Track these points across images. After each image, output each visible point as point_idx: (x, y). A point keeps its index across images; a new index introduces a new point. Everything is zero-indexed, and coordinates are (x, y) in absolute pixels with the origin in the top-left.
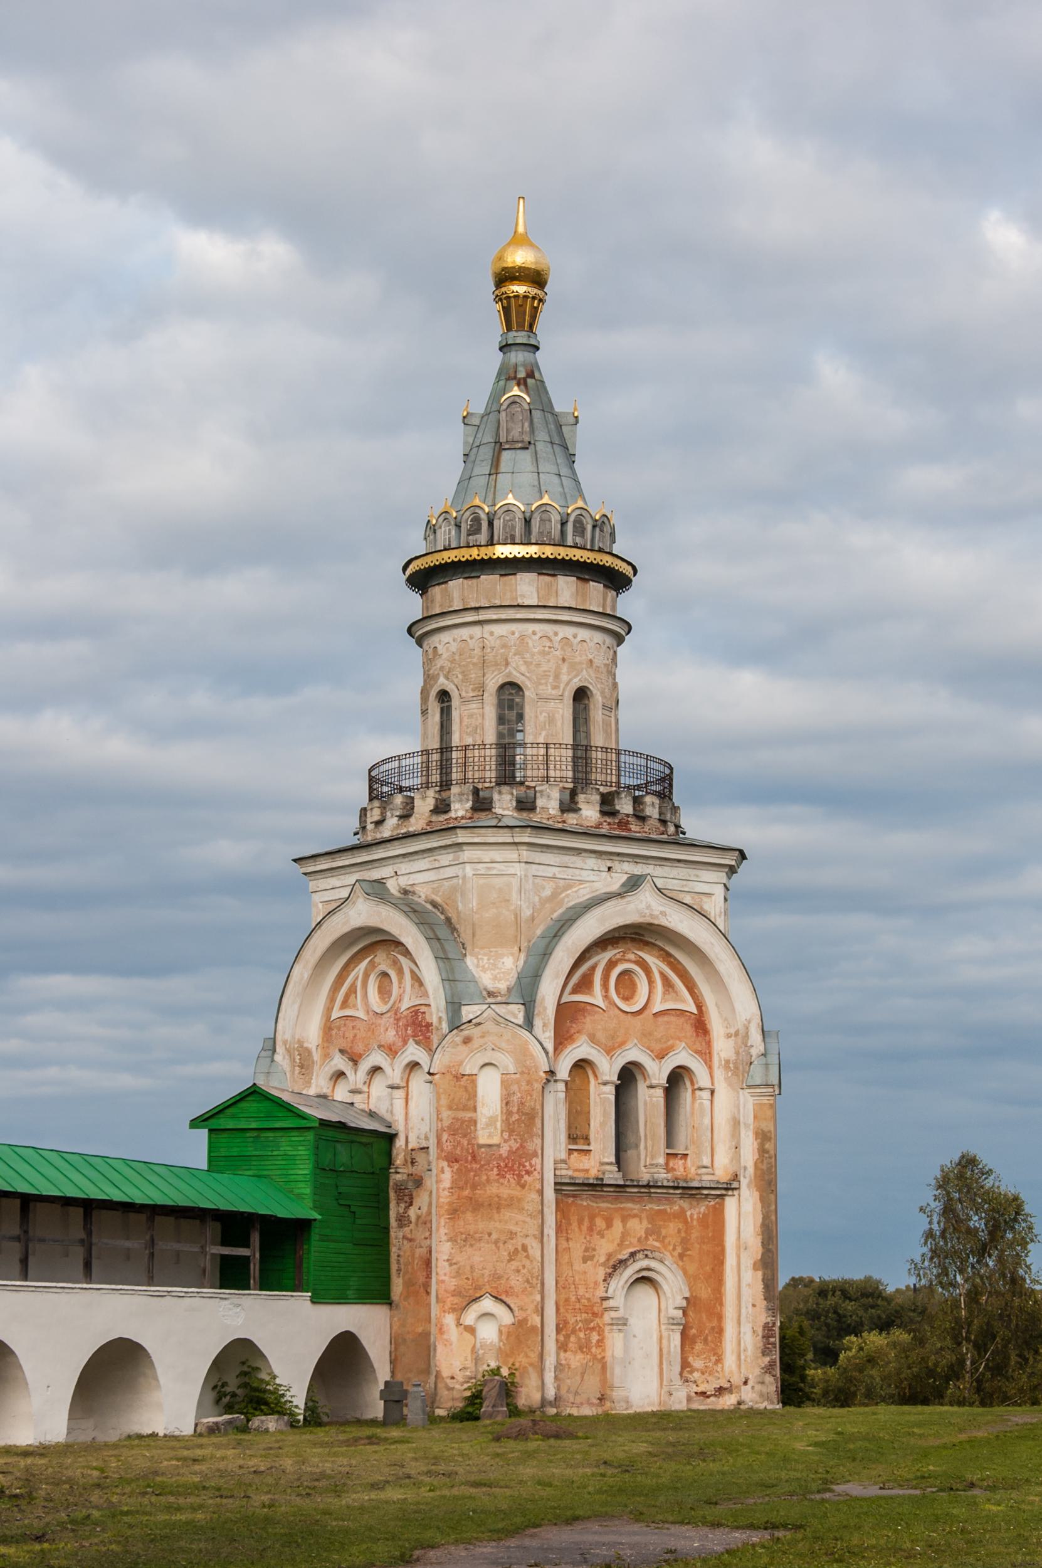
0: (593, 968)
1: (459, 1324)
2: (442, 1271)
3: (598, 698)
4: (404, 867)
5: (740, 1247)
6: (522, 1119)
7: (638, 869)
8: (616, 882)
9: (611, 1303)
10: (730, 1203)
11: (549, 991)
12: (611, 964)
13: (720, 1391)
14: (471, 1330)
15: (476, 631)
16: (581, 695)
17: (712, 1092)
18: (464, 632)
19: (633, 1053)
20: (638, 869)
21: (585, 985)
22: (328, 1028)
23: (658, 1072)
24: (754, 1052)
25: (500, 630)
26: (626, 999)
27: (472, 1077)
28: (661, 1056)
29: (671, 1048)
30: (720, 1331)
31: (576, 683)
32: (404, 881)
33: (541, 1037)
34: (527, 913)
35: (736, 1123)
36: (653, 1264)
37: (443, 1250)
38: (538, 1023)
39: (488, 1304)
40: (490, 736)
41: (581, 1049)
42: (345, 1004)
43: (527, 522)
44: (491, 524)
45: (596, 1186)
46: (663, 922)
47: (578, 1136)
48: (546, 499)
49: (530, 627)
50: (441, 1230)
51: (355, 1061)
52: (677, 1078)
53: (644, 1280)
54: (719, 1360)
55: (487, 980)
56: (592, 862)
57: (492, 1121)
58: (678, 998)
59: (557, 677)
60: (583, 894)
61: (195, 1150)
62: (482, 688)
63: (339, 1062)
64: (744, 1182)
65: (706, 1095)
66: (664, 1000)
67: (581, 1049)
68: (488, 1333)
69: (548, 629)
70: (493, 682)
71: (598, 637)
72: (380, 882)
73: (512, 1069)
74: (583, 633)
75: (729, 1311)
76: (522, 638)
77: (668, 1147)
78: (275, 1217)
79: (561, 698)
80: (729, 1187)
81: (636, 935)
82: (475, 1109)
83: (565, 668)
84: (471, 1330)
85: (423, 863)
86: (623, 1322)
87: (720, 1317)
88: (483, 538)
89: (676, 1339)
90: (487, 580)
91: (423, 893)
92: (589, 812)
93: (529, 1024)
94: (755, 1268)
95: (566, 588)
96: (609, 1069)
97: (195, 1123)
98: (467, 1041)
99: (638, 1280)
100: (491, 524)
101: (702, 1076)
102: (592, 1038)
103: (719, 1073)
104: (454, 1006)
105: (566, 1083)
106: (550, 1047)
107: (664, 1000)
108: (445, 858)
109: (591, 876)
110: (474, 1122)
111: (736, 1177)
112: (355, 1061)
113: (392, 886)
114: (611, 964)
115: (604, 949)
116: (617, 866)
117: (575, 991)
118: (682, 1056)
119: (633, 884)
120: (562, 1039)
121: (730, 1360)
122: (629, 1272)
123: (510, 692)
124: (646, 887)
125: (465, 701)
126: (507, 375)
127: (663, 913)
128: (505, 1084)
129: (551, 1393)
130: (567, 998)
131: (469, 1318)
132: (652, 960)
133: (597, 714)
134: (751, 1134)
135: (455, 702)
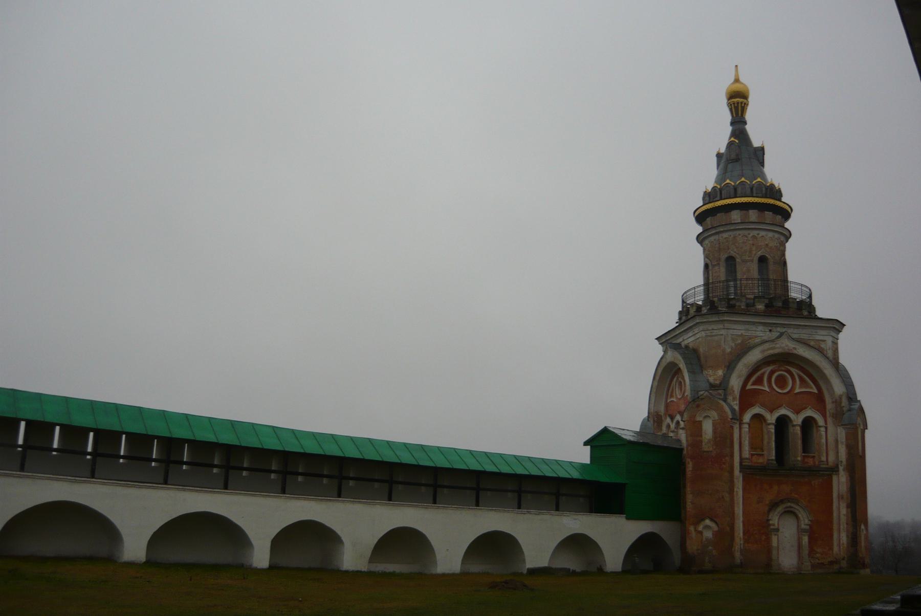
0: (763, 374)
1: (696, 530)
2: (689, 506)
3: (771, 261)
4: (685, 337)
5: (840, 497)
6: (723, 439)
7: (784, 330)
8: (775, 335)
9: (771, 522)
10: (835, 478)
11: (735, 383)
12: (772, 372)
13: (831, 563)
14: (701, 533)
15: (716, 237)
16: (762, 260)
17: (826, 428)
18: (712, 238)
19: (783, 411)
20: (784, 330)
21: (759, 381)
22: (667, 406)
23: (798, 419)
24: (845, 409)
25: (725, 235)
26: (782, 387)
27: (700, 422)
28: (797, 412)
29: (805, 408)
30: (831, 536)
31: (760, 253)
32: (686, 342)
33: (732, 403)
34: (729, 350)
35: (837, 441)
36: (792, 505)
37: (689, 498)
38: (730, 398)
39: (708, 522)
40: (723, 278)
41: (756, 410)
42: (672, 396)
43: (735, 189)
44: (721, 193)
45: (762, 470)
46: (795, 352)
47: (757, 446)
48: (743, 179)
49: (738, 232)
50: (688, 489)
51: (672, 418)
52: (808, 423)
53: (790, 512)
54: (831, 549)
55: (711, 379)
56: (761, 328)
57: (709, 441)
58: (808, 386)
59: (751, 251)
60: (757, 340)
61: (584, 456)
62: (720, 259)
63: (668, 420)
64: (841, 468)
65: (823, 429)
66: (800, 387)
67: (756, 410)
68: (708, 534)
69: (746, 232)
70: (724, 256)
71: (770, 234)
72: (679, 344)
73: (717, 418)
74: (762, 233)
75: (835, 527)
76: (735, 237)
77: (804, 451)
78: (598, 482)
79: (752, 261)
80: (834, 470)
81: (785, 359)
82: (701, 436)
83: (754, 248)
84: (701, 533)
85: (690, 334)
86: (777, 530)
87: (831, 530)
88: (718, 198)
89: (805, 539)
90: (720, 216)
91: (691, 346)
92: (760, 307)
93: (725, 400)
94: (848, 507)
95: (753, 215)
96: (771, 418)
97: (586, 444)
98: (698, 406)
99: (785, 512)
100: (721, 193)
101: (821, 421)
102: (763, 405)
103: (829, 420)
104: (695, 390)
105: (749, 425)
106: (737, 408)
107: (800, 387)
108: (696, 330)
109: (760, 333)
110: (701, 441)
111: (837, 466)
112: (672, 418)
113: (683, 345)
114: (772, 372)
115: (769, 365)
116: (774, 329)
117: (753, 384)
118: (809, 413)
119: (782, 334)
120: (745, 404)
121: (836, 549)
122: (780, 509)
123: (731, 260)
124: (784, 336)
125: (714, 266)
126: (733, 134)
127: (795, 349)
128: (714, 425)
129: (738, 561)
130: (749, 387)
131: (700, 528)
132: (794, 371)
133: (771, 267)
134: (844, 446)
135: (710, 268)
